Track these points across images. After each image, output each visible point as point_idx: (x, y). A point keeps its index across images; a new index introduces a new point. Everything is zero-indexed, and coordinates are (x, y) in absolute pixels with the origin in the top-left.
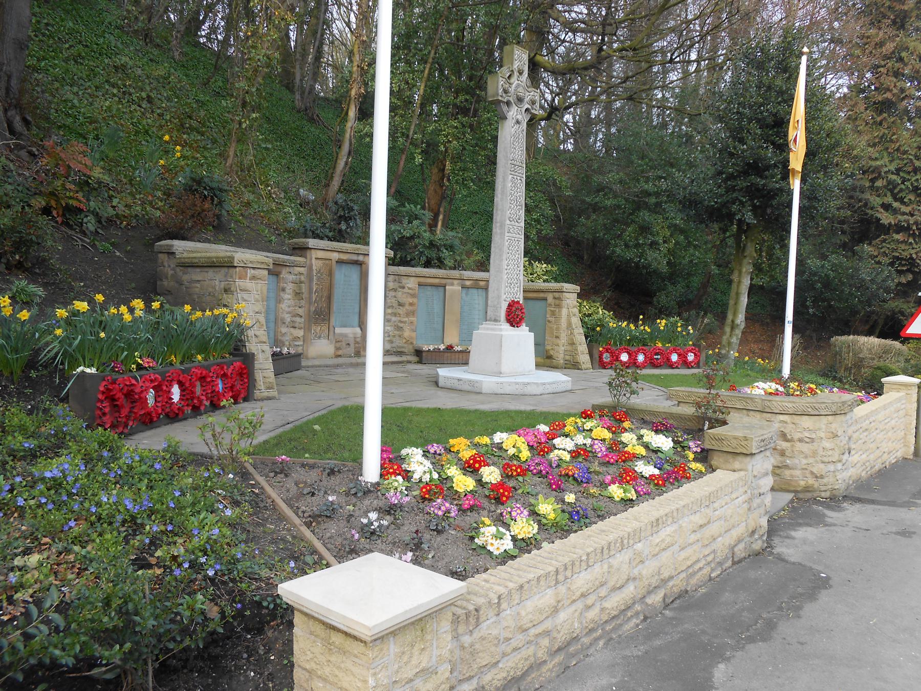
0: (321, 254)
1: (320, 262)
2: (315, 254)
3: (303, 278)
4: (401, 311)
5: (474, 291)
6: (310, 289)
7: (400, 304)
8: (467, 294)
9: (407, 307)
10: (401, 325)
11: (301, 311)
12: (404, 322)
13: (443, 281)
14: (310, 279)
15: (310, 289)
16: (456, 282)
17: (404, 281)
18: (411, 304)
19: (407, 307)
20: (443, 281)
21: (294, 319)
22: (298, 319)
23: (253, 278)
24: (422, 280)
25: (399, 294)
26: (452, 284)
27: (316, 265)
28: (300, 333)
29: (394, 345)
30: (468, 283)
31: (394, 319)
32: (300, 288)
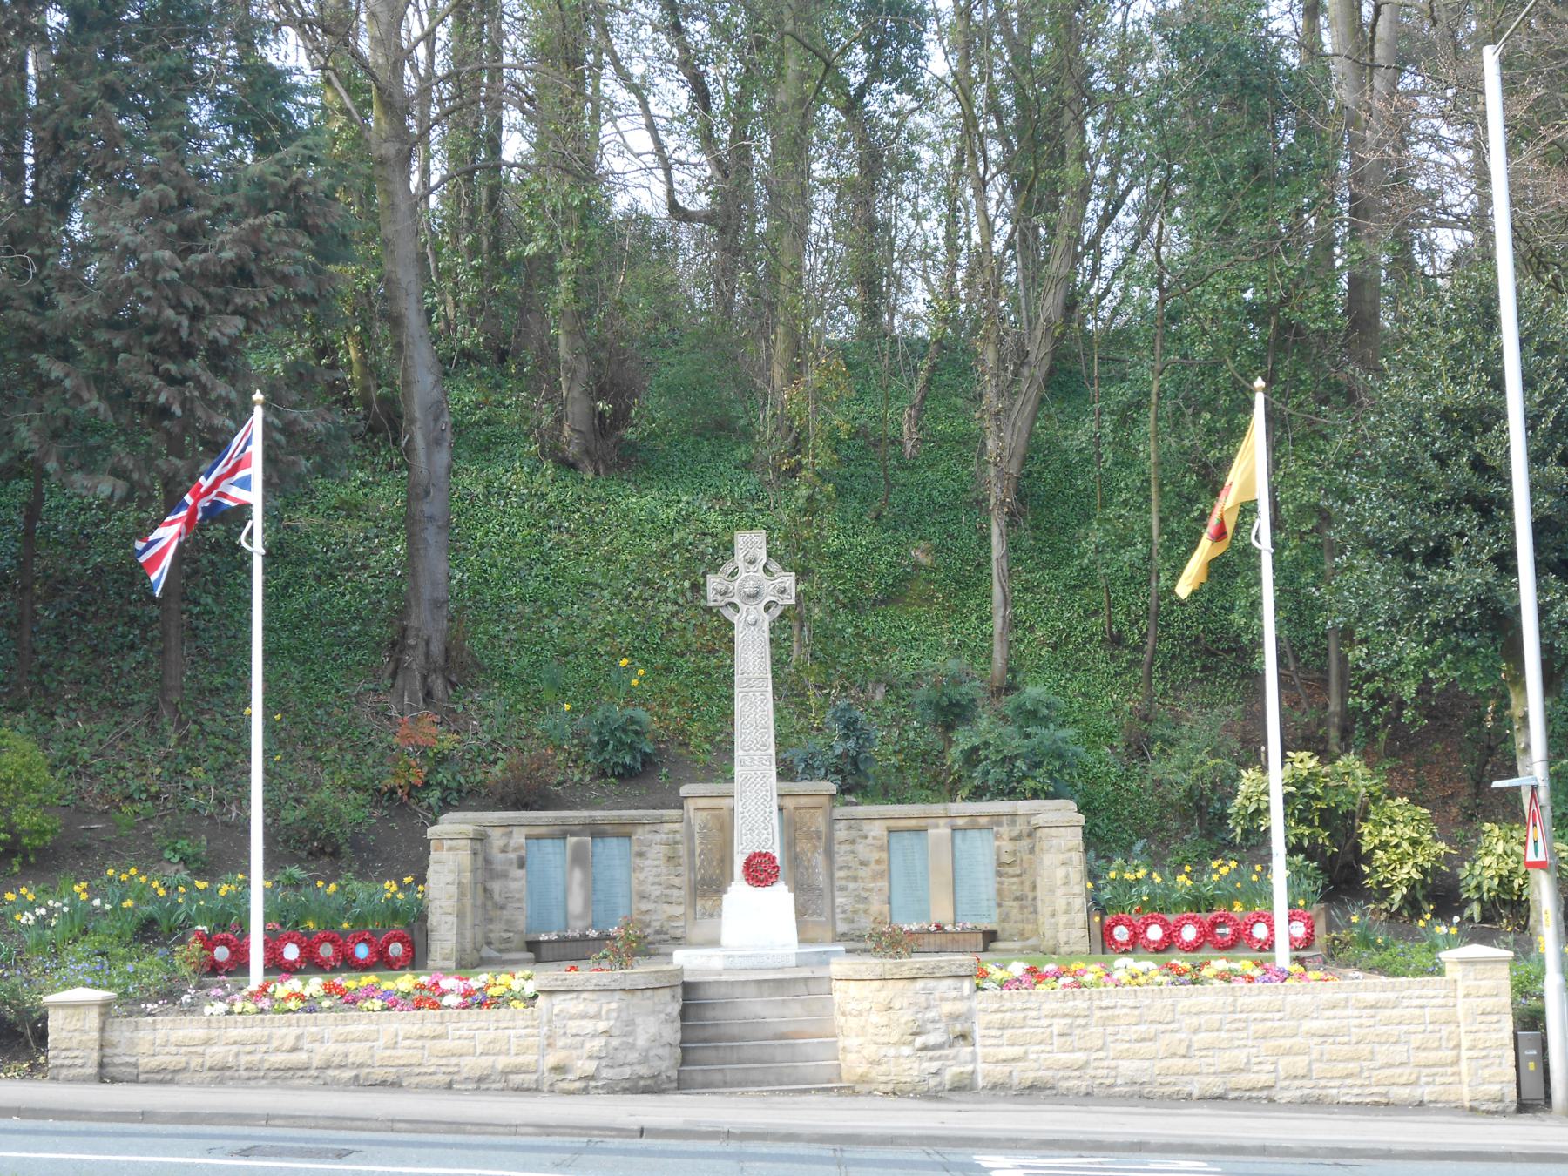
0: (702, 803)
1: (705, 813)
2: (690, 805)
3: (678, 837)
4: (864, 873)
5: (975, 834)
6: (691, 853)
7: (862, 863)
8: (964, 840)
9: (873, 866)
10: (864, 894)
11: (677, 882)
12: (871, 890)
13: (923, 823)
14: (691, 837)
15: (691, 853)
16: (941, 822)
17: (866, 826)
18: (878, 862)
19: (873, 866)
20: (923, 823)
21: (668, 892)
22: (675, 892)
23: (450, 849)
24: (891, 823)
25: (861, 848)
26: (937, 826)
27: (697, 820)
28: (679, 910)
29: (855, 926)
30: (960, 822)
31: (852, 885)
32: (675, 850)
